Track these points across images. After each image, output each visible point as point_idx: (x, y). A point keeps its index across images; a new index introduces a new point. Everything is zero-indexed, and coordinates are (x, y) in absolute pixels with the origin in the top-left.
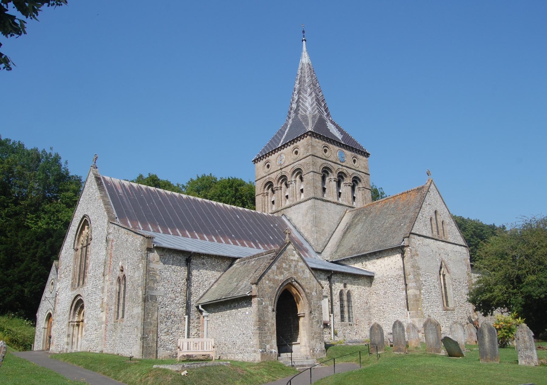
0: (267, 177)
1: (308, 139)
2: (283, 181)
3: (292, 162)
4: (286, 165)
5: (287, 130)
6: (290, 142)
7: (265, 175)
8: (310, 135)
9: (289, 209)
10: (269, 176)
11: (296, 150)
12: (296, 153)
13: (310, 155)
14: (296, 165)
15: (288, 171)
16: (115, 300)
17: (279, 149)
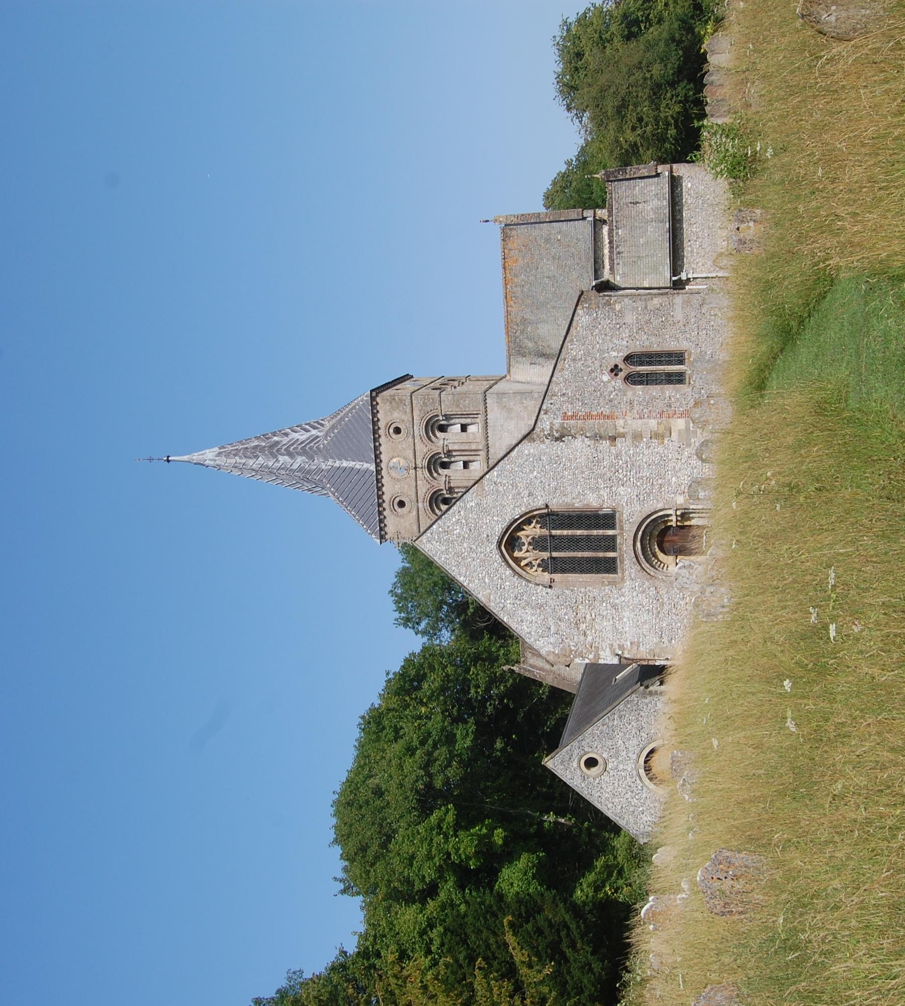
0: (420, 505)
1: (383, 399)
2: (437, 472)
3: (411, 440)
4: (411, 456)
5: (345, 464)
6: (375, 440)
7: (415, 513)
8: (377, 396)
9: (491, 450)
10: (420, 500)
11: (391, 431)
12: (398, 431)
13: (411, 396)
14: (419, 430)
15: (424, 450)
16: (654, 390)
17: (379, 472)
